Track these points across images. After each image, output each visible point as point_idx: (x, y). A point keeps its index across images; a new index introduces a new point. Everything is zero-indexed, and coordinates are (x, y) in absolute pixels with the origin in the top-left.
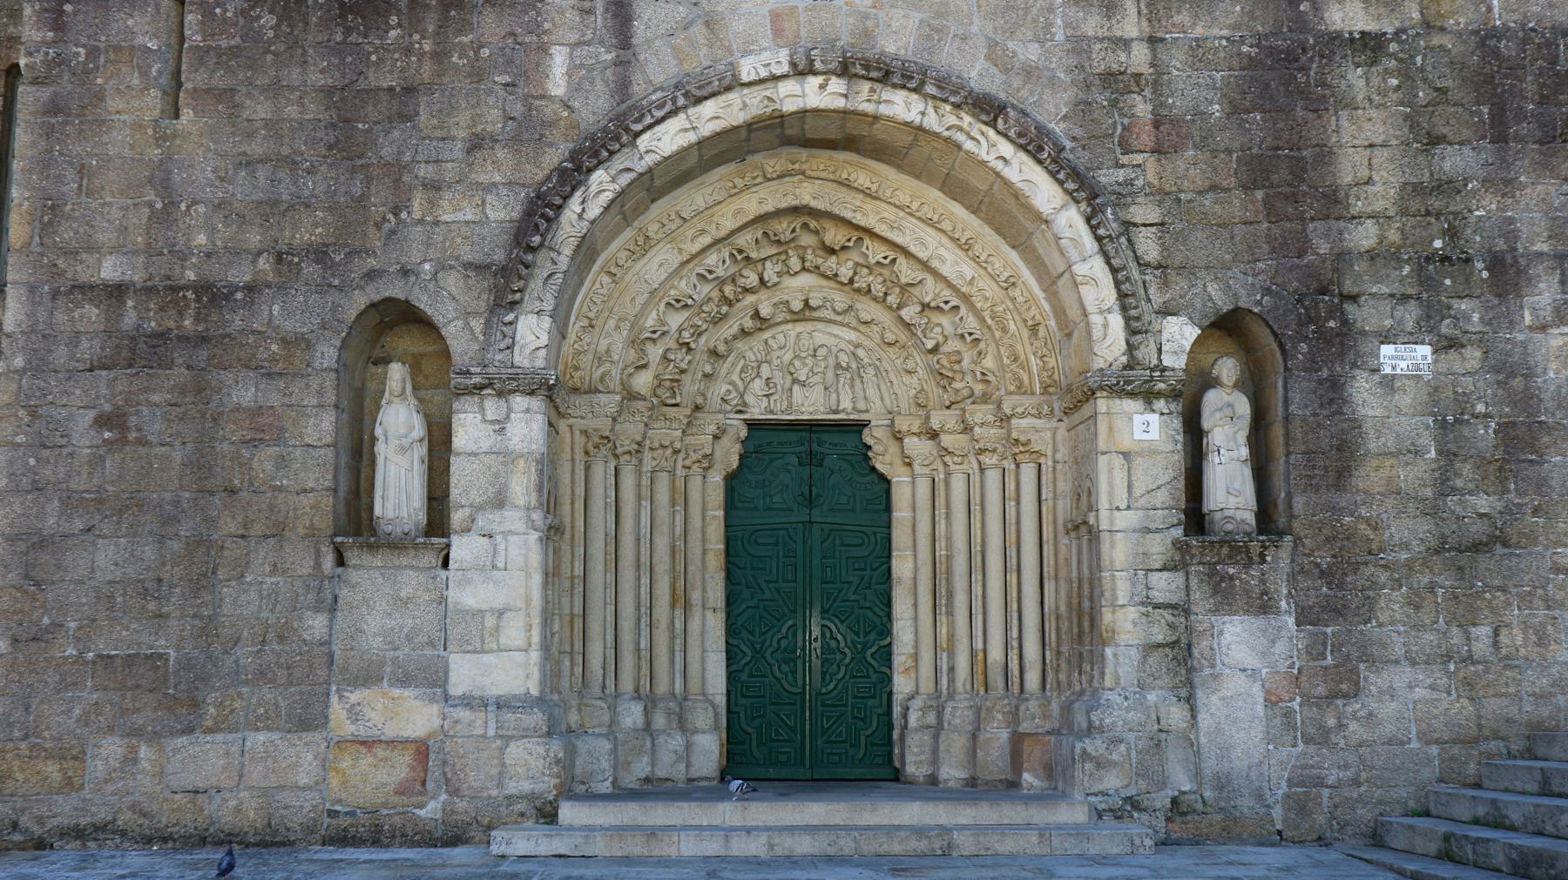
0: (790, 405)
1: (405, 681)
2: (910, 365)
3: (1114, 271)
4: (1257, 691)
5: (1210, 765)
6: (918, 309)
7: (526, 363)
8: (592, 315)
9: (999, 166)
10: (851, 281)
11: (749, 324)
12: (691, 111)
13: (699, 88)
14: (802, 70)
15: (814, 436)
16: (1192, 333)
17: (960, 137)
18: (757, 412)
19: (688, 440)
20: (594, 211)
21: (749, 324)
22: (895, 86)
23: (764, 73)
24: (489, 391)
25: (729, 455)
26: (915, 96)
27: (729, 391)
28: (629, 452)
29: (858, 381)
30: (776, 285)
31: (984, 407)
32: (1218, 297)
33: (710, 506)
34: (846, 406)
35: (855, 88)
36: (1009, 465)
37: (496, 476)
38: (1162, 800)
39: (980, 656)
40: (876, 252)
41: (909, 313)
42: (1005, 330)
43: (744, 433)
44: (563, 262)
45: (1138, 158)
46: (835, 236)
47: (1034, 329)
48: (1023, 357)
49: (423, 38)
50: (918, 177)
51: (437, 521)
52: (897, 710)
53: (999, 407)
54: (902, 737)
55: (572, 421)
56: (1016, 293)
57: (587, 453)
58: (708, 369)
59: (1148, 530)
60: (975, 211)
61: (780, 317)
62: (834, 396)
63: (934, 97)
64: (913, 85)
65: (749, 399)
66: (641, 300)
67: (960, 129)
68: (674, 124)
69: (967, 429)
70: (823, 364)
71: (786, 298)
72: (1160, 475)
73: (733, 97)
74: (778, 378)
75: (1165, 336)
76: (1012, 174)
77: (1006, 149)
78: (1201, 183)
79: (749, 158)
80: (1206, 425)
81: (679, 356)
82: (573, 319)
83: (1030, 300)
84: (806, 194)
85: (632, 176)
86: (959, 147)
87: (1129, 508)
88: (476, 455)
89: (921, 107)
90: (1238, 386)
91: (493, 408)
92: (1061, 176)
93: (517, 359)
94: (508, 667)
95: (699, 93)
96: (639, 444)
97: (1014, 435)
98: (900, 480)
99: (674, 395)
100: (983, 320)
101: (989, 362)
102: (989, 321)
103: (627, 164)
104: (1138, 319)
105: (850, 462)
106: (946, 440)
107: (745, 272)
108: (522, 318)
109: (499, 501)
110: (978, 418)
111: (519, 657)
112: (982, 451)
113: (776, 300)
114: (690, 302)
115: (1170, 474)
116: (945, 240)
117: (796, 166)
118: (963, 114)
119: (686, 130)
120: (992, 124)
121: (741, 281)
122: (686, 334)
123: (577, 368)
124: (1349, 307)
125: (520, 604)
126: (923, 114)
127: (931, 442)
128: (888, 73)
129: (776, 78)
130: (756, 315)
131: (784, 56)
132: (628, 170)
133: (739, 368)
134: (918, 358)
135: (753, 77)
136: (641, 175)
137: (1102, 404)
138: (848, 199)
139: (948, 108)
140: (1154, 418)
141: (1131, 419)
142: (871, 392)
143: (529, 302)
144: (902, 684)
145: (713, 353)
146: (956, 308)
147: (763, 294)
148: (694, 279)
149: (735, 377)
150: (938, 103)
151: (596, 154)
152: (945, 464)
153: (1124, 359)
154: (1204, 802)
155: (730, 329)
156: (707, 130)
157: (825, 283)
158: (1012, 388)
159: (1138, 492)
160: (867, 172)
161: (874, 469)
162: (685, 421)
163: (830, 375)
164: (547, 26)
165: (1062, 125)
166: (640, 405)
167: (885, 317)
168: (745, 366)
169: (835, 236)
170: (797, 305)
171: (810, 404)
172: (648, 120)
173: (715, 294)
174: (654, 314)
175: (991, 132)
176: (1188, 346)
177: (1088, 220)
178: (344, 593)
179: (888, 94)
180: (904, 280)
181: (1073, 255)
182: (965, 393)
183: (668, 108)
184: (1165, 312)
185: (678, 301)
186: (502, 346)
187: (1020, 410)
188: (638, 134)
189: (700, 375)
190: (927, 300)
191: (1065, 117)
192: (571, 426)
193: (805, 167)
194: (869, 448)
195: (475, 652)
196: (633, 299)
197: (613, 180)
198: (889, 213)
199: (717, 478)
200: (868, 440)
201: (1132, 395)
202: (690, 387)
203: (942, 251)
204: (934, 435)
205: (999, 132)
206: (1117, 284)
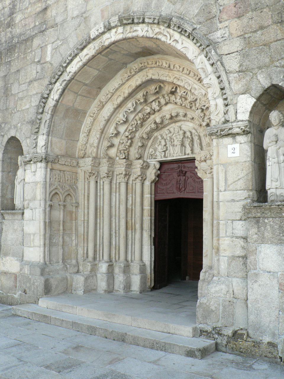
1: (13, 256)
3: (219, 77)
4: (275, 282)
5: (252, 317)
7: (40, 152)
8: (86, 132)
9: (173, 44)
12: (80, 54)
14: (109, 28)
16: (252, 101)
17: (160, 37)
18: (160, 157)
20: (56, 97)
21: (153, 126)
23: (97, 33)
24: (31, 162)
25: (151, 174)
26: (144, 25)
27: (152, 151)
28: (105, 177)
32: (263, 81)
35: (125, 29)
37: (33, 190)
38: (229, 332)
43: (158, 166)
44: (49, 116)
45: (227, 23)
49: (22, 54)
55: (81, 168)
57: (87, 179)
59: (233, 201)
63: (149, 23)
64: (141, 21)
67: (160, 33)
71: (164, 114)
73: (91, 46)
75: (239, 105)
76: (179, 47)
77: (177, 36)
78: (255, 26)
79: (128, 66)
80: (265, 147)
81: (125, 142)
82: (81, 134)
84: (151, 74)
85: (65, 82)
87: (225, 190)
88: (29, 183)
89: (146, 28)
91: (33, 166)
92: (195, 41)
93: (39, 151)
94: (35, 253)
95: (80, 47)
103: (64, 79)
107: (145, 107)
109: (34, 199)
111: (38, 249)
113: (161, 116)
115: (245, 172)
117: (143, 65)
119: (79, 62)
120: (169, 27)
125: (38, 232)
128: (133, 20)
130: (155, 123)
131: (102, 26)
132: (65, 80)
135: (94, 36)
136: (69, 81)
139: (156, 26)
140: (237, 146)
141: (227, 148)
143: (41, 132)
147: (157, 114)
150: (152, 25)
153: (223, 119)
156: (84, 60)
159: (229, 182)
164: (47, 39)
165: (195, 19)
170: (168, 116)
171: (175, 154)
172: (67, 61)
175: (171, 31)
176: (250, 109)
178: (4, 227)
179: (135, 28)
186: (33, 147)
188: (66, 67)
191: (196, 16)
192: (81, 170)
195: (29, 247)
197: (61, 85)
198: (177, 74)
199: (147, 183)
203: (195, 86)
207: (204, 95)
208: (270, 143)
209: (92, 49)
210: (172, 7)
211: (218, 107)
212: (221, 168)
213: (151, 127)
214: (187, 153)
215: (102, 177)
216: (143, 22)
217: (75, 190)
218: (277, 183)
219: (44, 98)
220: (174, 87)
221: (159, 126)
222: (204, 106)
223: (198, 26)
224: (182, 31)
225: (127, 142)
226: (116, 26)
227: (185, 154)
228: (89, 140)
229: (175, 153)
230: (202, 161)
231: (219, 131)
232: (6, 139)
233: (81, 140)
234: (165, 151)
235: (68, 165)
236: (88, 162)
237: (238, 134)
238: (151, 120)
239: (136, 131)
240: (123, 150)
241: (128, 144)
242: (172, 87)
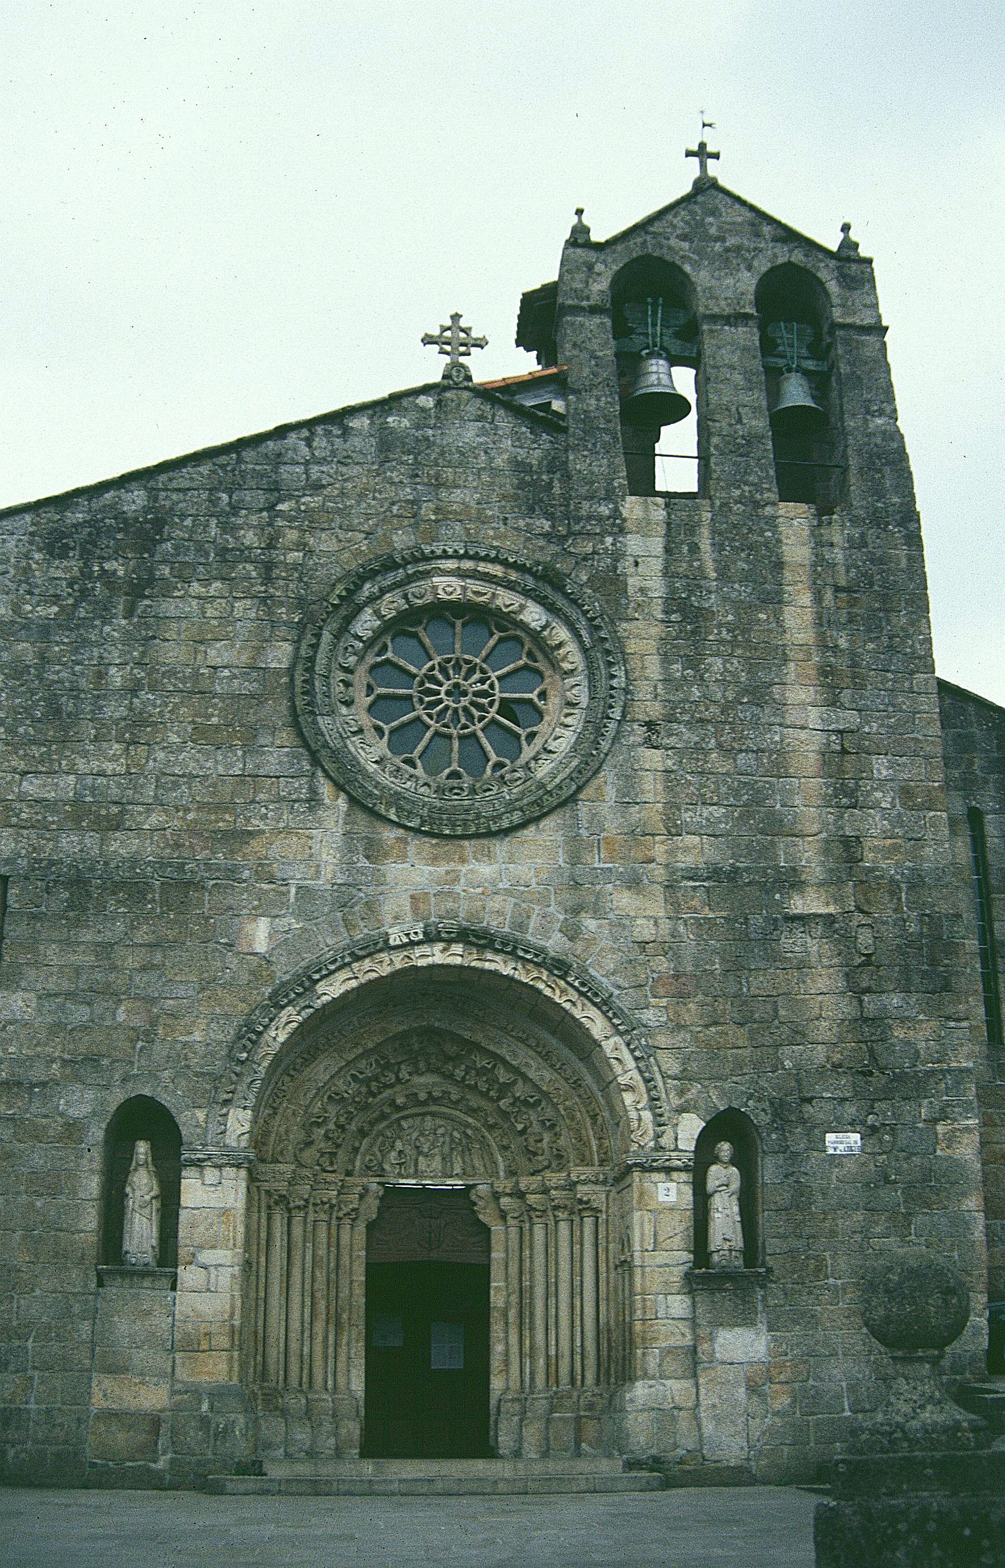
0: (416, 1171)
3: (647, 1081)
6: (511, 1101)
9: (567, 1006)
10: (463, 1078)
13: (360, 949)
14: (430, 938)
17: (541, 986)
22: (497, 951)
23: (406, 940)
25: (371, 1208)
27: (371, 1160)
28: (298, 1207)
33: (355, 1247)
36: (576, 1219)
39: (553, 1361)
45: (664, 1002)
46: (452, 1049)
47: (594, 1118)
48: (585, 1138)
51: (168, 1251)
52: (493, 1402)
53: (569, 1175)
54: (496, 1422)
56: (581, 1091)
60: (553, 1033)
65: (387, 1167)
66: (310, 1095)
68: (342, 975)
69: (546, 1191)
70: (441, 1139)
72: (677, 1230)
74: (408, 1150)
75: (680, 1128)
76: (577, 1013)
77: (574, 996)
83: (592, 1097)
86: (539, 992)
90: (733, 1162)
92: (610, 1014)
95: (361, 953)
96: (306, 1200)
97: (578, 1196)
98: (497, 1228)
99: (332, 1164)
101: (562, 1142)
104: (661, 1115)
106: (532, 1199)
108: (232, 1111)
112: (556, 1208)
114: (346, 1095)
116: (531, 1053)
118: (543, 970)
120: (562, 977)
122: (342, 1119)
123: (264, 1144)
124: (807, 1108)
126: (515, 969)
129: (413, 944)
130: (392, 1103)
133: (378, 1143)
144: (497, 1383)
146: (538, 1102)
147: (398, 1088)
148: (349, 1079)
149: (376, 1149)
151: (286, 996)
152: (531, 1218)
154: (703, 1457)
158: (578, 1161)
161: (479, 1220)
162: (340, 1184)
163: (446, 1149)
168: (383, 1144)
170: (423, 1096)
172: (324, 972)
173: (364, 1089)
174: (319, 1104)
175: (562, 983)
176: (696, 1137)
177: (628, 1045)
180: (501, 1080)
181: (618, 1069)
182: (546, 1163)
183: (338, 964)
184: (681, 1110)
185: (337, 1094)
187: (582, 1177)
194: (475, 1204)
196: (305, 1094)
201: (658, 1170)
202: (342, 1156)
205: (568, 983)
206: (649, 1090)
208: (720, 1186)
209: (385, 964)
210: (569, 944)
211: (642, 1124)
212: (647, 1216)
215: (292, 1205)
216: (513, 953)
218: (731, 1244)
219: (254, 1031)
223: (617, 992)
224: (589, 992)
226: (450, 942)
232: (117, 1097)
234: (400, 1164)
237: (677, 1169)
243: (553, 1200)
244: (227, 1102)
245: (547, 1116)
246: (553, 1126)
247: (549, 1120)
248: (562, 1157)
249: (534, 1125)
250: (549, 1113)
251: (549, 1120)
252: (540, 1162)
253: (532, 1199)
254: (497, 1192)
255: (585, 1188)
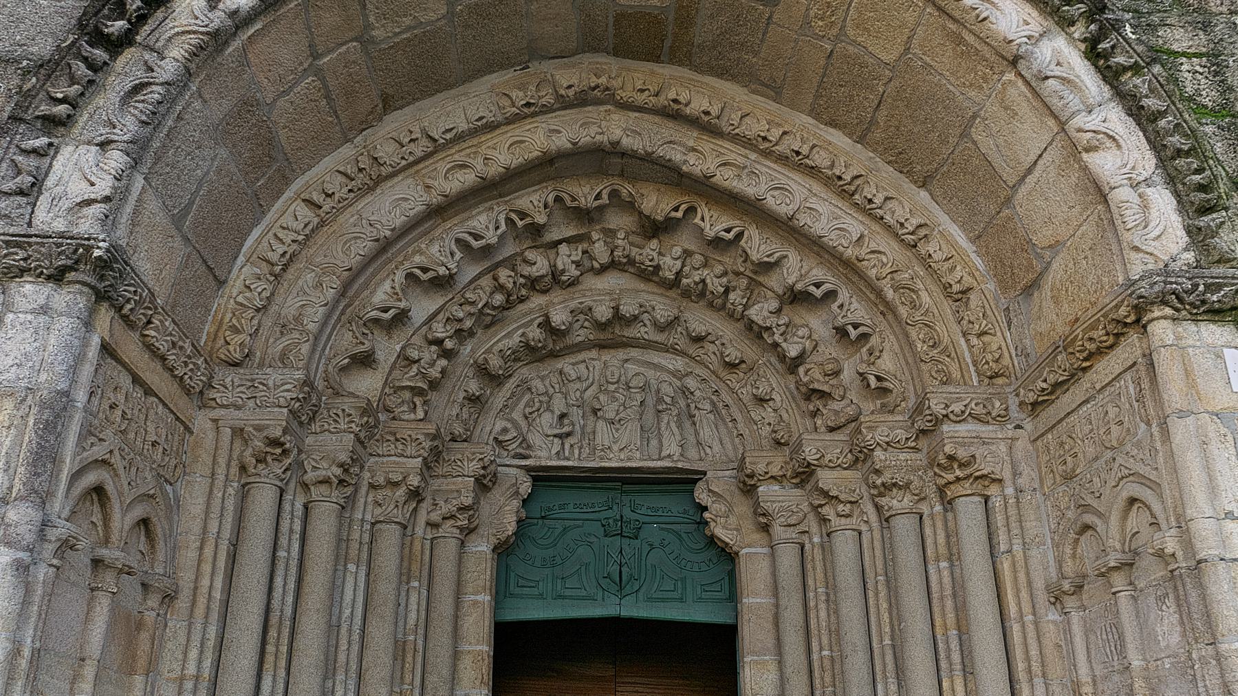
2: (762, 390)
6: (774, 305)
11: (535, 333)
15: (626, 500)
19: (436, 484)
21: (535, 333)
29: (687, 424)
30: (574, 283)
31: (890, 418)
34: (669, 451)
40: (714, 222)
41: (760, 312)
42: (914, 306)
48: (946, 340)
50: (777, 99)
56: (931, 248)
58: (473, 387)
61: (580, 335)
62: (654, 442)
71: (588, 302)
97: (948, 449)
100: (879, 294)
101: (887, 363)
102: (890, 294)
105: (677, 534)
106: (826, 478)
107: (530, 255)
110: (881, 435)
112: (888, 487)
113: (573, 304)
116: (817, 187)
121: (526, 270)
123: (236, 330)
127: (798, 492)
130: (546, 324)
134: (773, 382)
137: (1162, 330)
138: (677, 137)
142: (706, 433)
145: (482, 371)
146: (831, 295)
147: (557, 295)
149: (517, 415)
155: (507, 338)
157: (642, 286)
160: (701, 94)
163: (649, 416)
166: (347, 404)
167: (725, 330)
169: (656, 203)
170: (603, 312)
171: (619, 448)
173: (486, 282)
180: (755, 256)
182: (851, 411)
185: (425, 270)
187: (957, 407)
189: (462, 395)
190: (791, 281)
193: (615, 84)
200: (701, 496)
203: (813, 203)
204: (804, 475)
207: (855, 239)
211: (1154, 214)
213: (523, 335)
214: (663, 454)
217: (174, 507)
220: (684, 207)
221: (551, 345)
222: (818, 285)
225: (432, 364)
227: (660, 459)
228: (278, 299)
229: (615, 448)
230: (772, 477)
231: (1201, 288)
233: (235, 285)
235: (171, 370)
236: (276, 387)
238: (531, 311)
239: (471, 333)
240: (412, 388)
241: (435, 373)
242: (674, 203)
243: (878, 472)
244: (52, 123)
245: (851, 318)
246: (864, 337)
247: (856, 326)
248: (886, 391)
249: (821, 348)
250: (855, 309)
251: (856, 326)
252: (836, 413)
253: (826, 478)
254: (751, 476)
255: (963, 429)
